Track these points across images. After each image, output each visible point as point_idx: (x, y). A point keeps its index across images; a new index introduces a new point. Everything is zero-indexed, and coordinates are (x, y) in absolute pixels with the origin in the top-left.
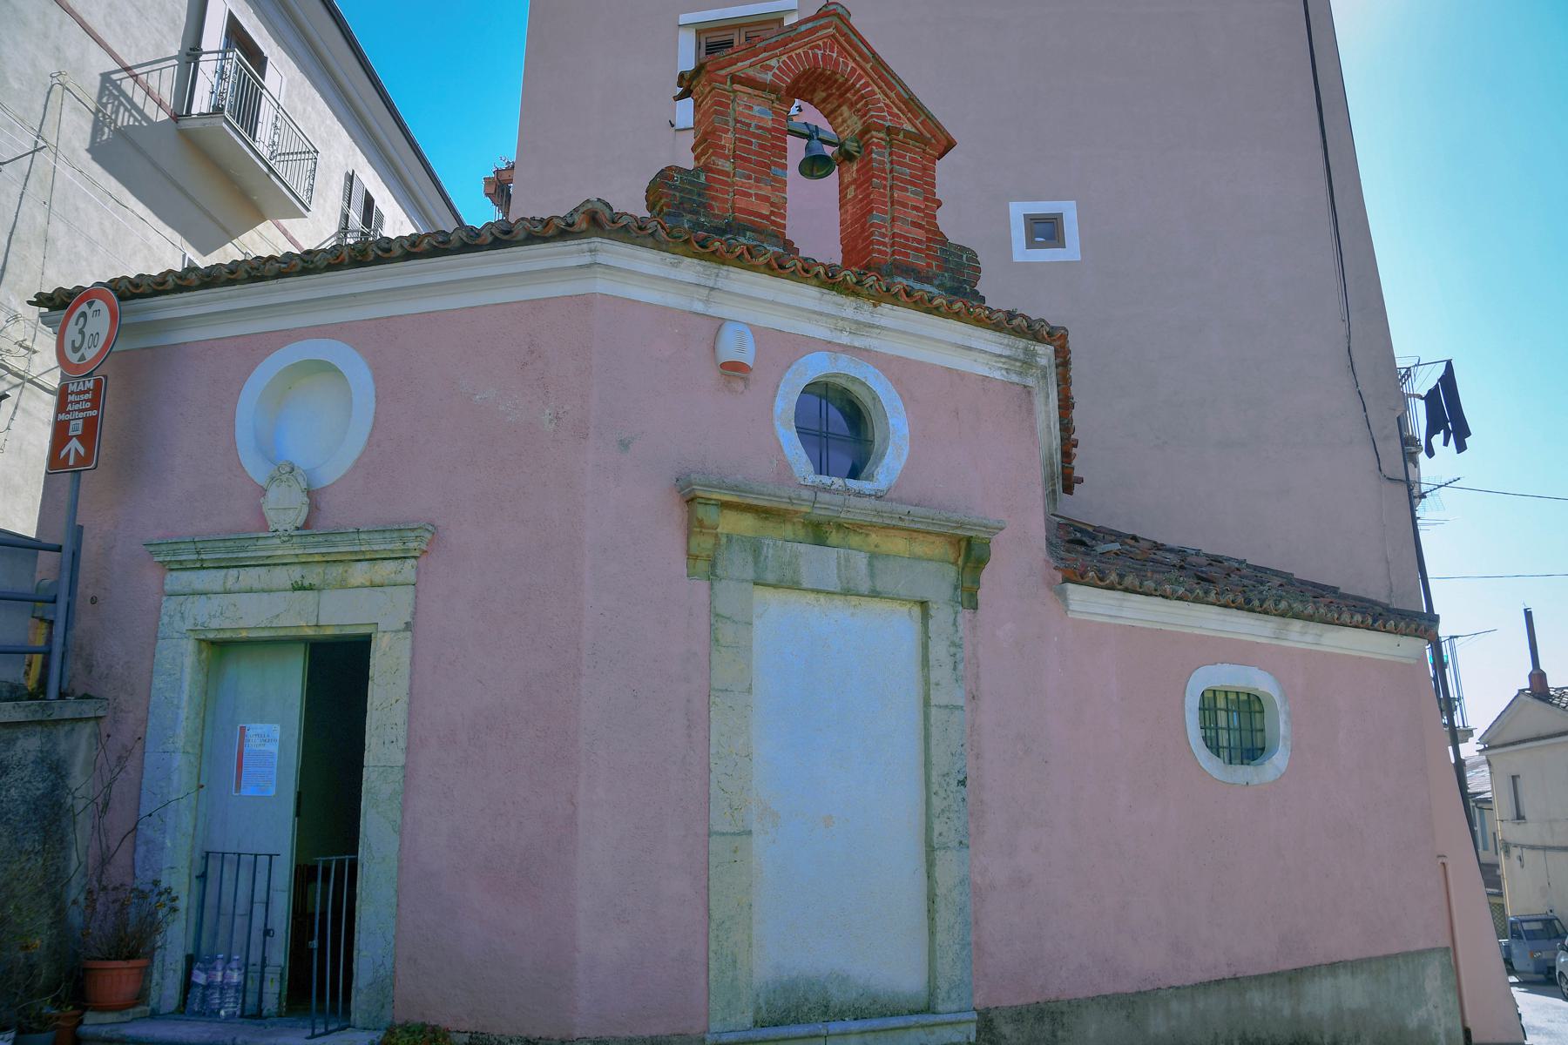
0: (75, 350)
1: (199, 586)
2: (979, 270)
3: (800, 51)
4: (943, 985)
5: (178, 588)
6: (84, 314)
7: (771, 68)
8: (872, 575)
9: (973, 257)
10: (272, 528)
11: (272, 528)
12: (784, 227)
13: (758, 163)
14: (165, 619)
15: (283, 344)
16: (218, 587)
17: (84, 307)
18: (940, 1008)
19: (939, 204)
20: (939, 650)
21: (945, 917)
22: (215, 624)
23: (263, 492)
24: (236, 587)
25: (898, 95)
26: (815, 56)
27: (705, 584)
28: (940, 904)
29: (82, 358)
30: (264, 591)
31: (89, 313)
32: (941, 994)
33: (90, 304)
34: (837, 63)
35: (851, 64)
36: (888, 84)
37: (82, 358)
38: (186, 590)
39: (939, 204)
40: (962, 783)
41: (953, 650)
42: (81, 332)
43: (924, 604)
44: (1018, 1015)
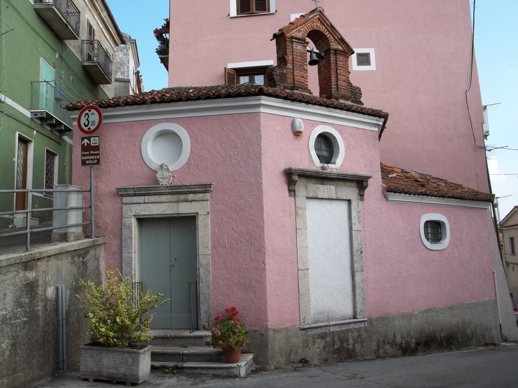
0: (86, 126)
1: (135, 201)
2: (361, 94)
3: (309, 24)
4: (358, 311)
5: (128, 202)
6: (87, 114)
7: (301, 31)
8: (336, 193)
9: (360, 90)
10: (161, 184)
11: (161, 184)
12: (307, 85)
13: (300, 65)
14: (125, 212)
15: (155, 124)
16: (142, 201)
17: (87, 111)
18: (358, 317)
19: (350, 73)
20: (354, 214)
21: (358, 291)
22: (143, 213)
23: (156, 172)
24: (149, 201)
25: (338, 37)
26: (314, 25)
27: (293, 198)
28: (357, 287)
29: (89, 129)
30: (158, 203)
31: (90, 114)
32: (358, 313)
33: (90, 111)
34: (320, 27)
35: (324, 27)
36: (335, 33)
37: (89, 129)
38: (131, 202)
39: (350, 73)
40: (361, 252)
41: (358, 214)
42: (87, 120)
43: (349, 201)
44: (378, 319)
